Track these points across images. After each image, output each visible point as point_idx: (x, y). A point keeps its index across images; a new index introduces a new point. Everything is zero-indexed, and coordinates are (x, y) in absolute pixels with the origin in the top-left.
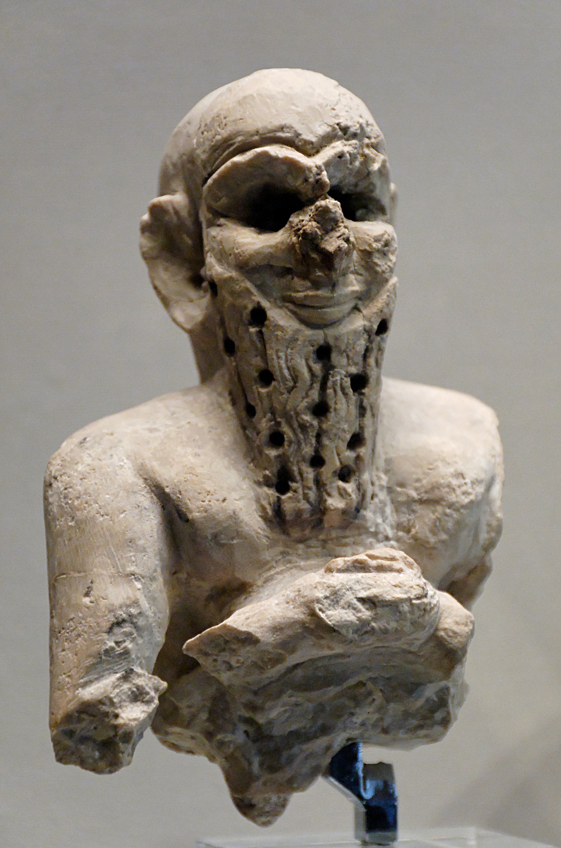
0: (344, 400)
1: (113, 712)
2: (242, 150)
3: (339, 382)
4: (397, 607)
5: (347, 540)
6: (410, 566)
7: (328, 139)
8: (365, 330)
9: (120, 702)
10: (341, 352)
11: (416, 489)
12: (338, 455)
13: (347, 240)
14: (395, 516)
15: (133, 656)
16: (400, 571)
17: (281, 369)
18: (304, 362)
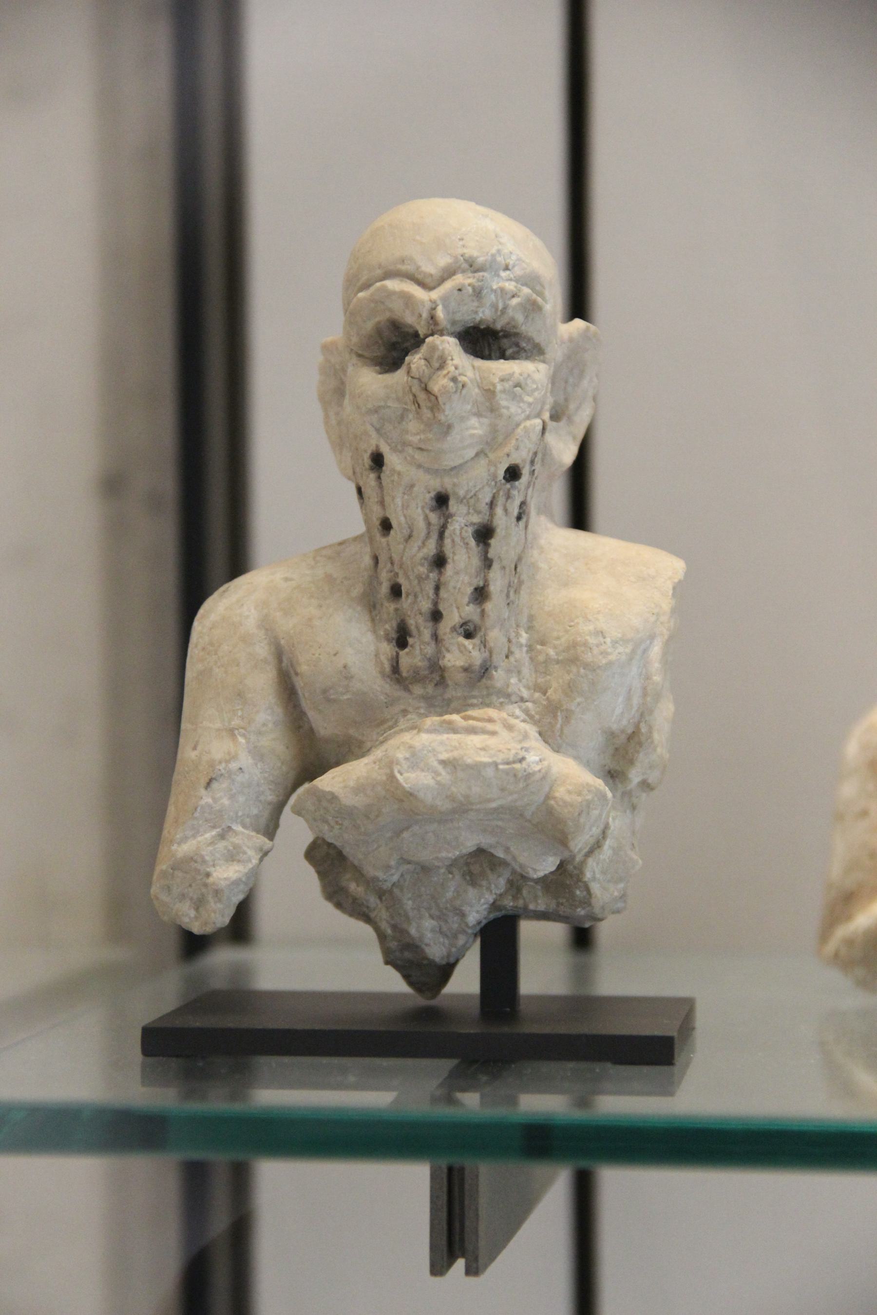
3: (458, 532)
7: (448, 273)
9: (214, 861)
11: (555, 647)
13: (454, 380)
14: (534, 676)
16: (493, 733)
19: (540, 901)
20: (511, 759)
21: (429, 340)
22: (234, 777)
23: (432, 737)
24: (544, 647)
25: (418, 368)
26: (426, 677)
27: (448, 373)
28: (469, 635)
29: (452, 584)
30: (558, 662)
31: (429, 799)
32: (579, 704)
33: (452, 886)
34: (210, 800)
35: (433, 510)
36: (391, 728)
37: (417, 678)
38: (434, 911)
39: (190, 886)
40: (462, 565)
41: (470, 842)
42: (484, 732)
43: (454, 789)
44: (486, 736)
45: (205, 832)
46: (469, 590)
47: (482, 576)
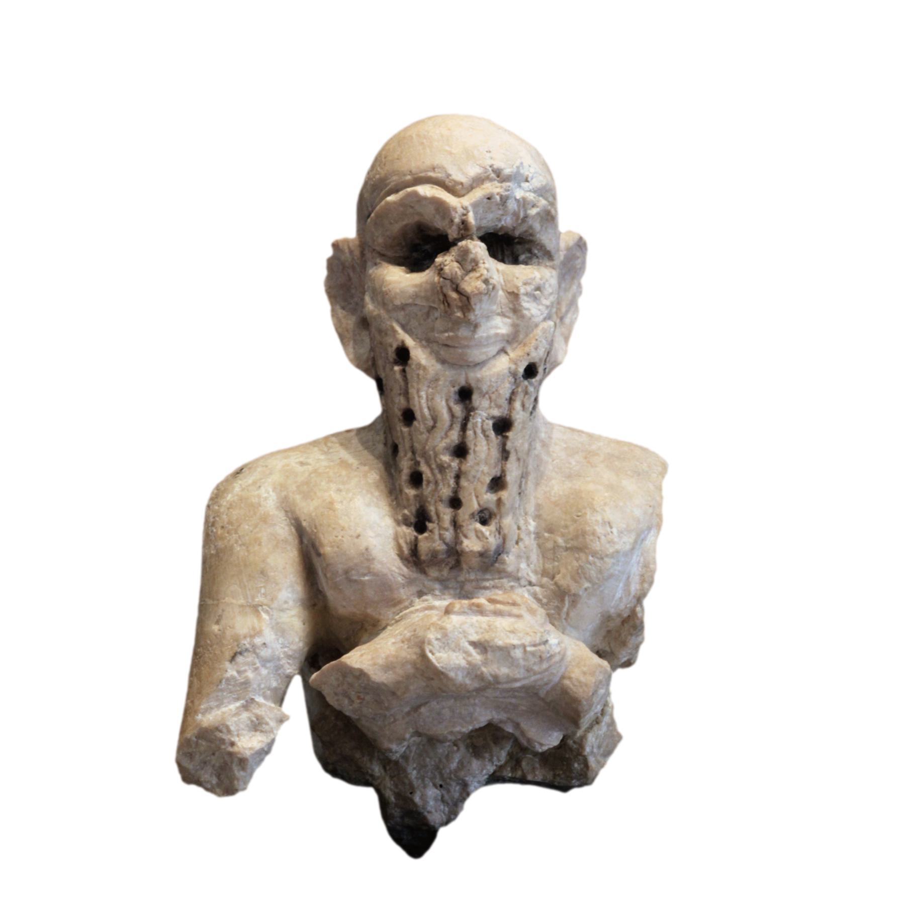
0: (484, 442)
1: (229, 740)
2: (396, 191)
3: (479, 425)
4: (509, 653)
5: (487, 584)
6: (532, 612)
7: (478, 181)
8: (510, 372)
9: (238, 730)
10: (483, 395)
11: (563, 535)
12: (477, 497)
13: (486, 281)
14: (541, 561)
15: (255, 686)
16: (519, 616)
17: (421, 409)
18: (444, 403)
19: (537, 773)
20: (538, 642)
21: (462, 244)
22: (258, 651)
23: (462, 618)
24: (552, 536)
25: (450, 270)
26: (442, 561)
27: (482, 275)
28: (484, 522)
29: (473, 473)
30: (567, 549)
31: (460, 677)
32: (586, 589)
33: (457, 758)
34: (235, 673)
35: (457, 403)
36: (406, 608)
37: (434, 559)
38: (439, 782)
39: (214, 754)
40: (483, 456)
41: (483, 717)
42: (510, 615)
43: (484, 669)
44: (512, 620)
45: (229, 703)
46: (488, 480)
47: (500, 467)
